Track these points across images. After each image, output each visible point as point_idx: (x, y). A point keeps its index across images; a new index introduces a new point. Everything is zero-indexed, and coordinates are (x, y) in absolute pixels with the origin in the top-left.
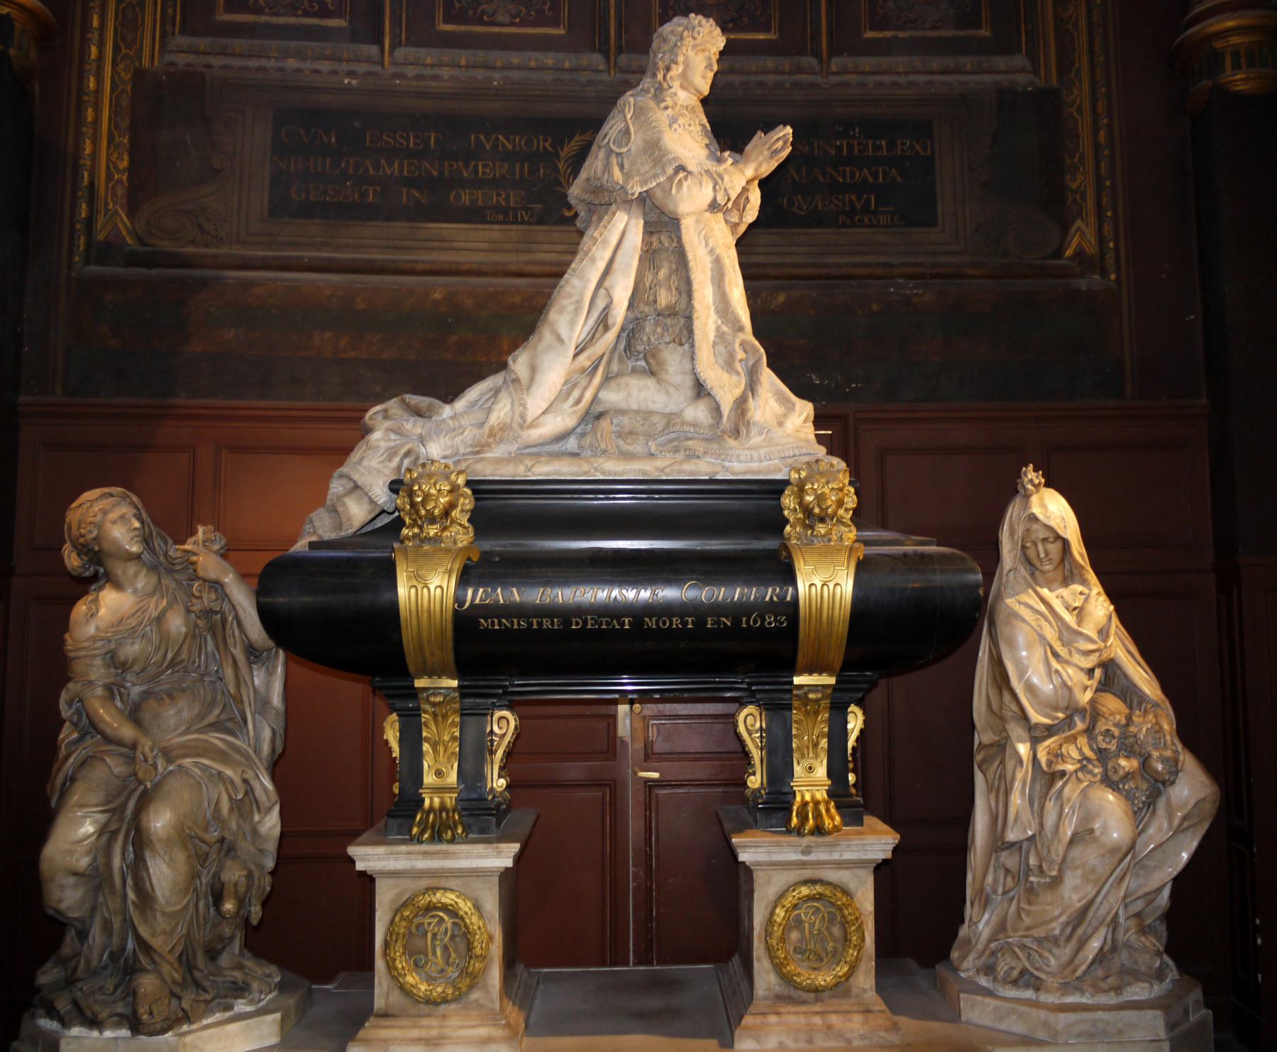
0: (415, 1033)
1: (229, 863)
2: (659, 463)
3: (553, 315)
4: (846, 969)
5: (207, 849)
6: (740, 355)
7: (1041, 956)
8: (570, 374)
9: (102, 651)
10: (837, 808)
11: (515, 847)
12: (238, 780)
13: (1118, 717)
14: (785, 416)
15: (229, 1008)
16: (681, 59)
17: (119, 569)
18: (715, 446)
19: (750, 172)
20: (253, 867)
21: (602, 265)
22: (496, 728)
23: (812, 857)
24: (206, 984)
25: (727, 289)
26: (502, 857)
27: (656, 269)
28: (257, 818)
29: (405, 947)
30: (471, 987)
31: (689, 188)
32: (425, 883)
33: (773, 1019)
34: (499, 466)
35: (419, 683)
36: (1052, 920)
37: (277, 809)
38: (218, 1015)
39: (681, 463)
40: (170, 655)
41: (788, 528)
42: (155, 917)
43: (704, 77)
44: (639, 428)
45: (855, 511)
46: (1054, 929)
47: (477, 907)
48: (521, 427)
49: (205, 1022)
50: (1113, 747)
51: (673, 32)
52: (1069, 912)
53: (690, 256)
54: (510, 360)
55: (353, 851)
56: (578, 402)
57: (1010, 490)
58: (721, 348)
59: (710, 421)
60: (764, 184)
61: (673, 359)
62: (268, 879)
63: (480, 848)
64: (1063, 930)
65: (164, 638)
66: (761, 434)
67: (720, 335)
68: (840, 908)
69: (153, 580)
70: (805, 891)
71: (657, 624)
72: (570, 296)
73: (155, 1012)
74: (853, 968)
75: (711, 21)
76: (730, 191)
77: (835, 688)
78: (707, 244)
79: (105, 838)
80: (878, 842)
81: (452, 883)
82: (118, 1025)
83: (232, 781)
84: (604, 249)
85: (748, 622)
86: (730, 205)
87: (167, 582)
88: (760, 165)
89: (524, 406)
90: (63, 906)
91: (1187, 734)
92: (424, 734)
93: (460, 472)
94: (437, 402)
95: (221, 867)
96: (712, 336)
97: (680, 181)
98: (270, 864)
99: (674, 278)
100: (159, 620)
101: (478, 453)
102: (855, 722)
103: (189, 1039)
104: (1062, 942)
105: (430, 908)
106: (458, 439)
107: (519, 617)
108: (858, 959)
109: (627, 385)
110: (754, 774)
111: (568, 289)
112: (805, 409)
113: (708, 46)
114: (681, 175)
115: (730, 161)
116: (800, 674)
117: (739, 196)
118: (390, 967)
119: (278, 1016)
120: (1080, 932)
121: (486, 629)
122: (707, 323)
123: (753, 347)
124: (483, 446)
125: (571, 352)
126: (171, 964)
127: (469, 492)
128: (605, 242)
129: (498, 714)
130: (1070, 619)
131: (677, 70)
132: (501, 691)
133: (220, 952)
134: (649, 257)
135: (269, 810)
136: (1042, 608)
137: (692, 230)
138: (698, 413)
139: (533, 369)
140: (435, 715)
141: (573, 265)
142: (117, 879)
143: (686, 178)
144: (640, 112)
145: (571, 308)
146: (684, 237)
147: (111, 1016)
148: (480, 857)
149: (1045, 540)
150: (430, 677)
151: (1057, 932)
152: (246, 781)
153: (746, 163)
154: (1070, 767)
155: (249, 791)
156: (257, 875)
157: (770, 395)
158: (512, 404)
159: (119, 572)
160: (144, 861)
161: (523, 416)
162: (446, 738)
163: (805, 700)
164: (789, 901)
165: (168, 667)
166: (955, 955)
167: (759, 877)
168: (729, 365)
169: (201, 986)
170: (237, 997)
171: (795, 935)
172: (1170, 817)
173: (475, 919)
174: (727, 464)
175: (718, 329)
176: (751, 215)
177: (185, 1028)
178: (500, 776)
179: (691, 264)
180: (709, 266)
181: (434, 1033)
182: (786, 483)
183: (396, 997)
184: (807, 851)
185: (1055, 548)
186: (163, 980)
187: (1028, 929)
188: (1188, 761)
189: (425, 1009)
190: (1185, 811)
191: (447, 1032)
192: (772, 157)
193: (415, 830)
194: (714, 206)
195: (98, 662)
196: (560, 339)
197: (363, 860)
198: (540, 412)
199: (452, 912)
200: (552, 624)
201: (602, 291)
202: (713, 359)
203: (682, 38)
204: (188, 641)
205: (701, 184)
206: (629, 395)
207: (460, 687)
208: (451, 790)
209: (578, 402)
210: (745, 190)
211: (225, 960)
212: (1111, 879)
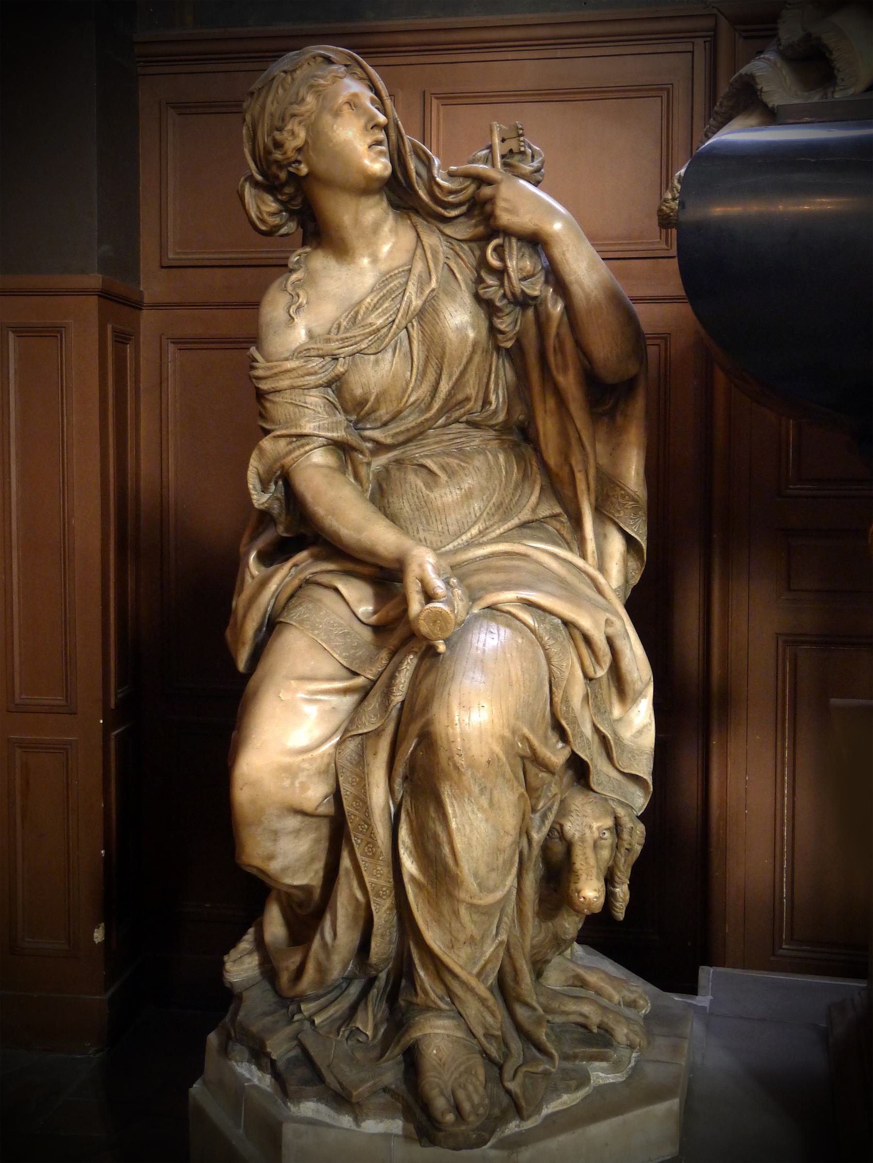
1: (579, 802)
9: (322, 378)
20: (621, 812)
24: (542, 1034)
38: (565, 1097)
40: (444, 387)
65: (435, 351)
69: (407, 237)
82: (384, 1112)
87: (431, 239)
95: (564, 811)
100: (427, 314)
126: (482, 1001)
147: (374, 1093)
159: (347, 219)
165: (440, 413)
195: (314, 399)
204: (477, 358)
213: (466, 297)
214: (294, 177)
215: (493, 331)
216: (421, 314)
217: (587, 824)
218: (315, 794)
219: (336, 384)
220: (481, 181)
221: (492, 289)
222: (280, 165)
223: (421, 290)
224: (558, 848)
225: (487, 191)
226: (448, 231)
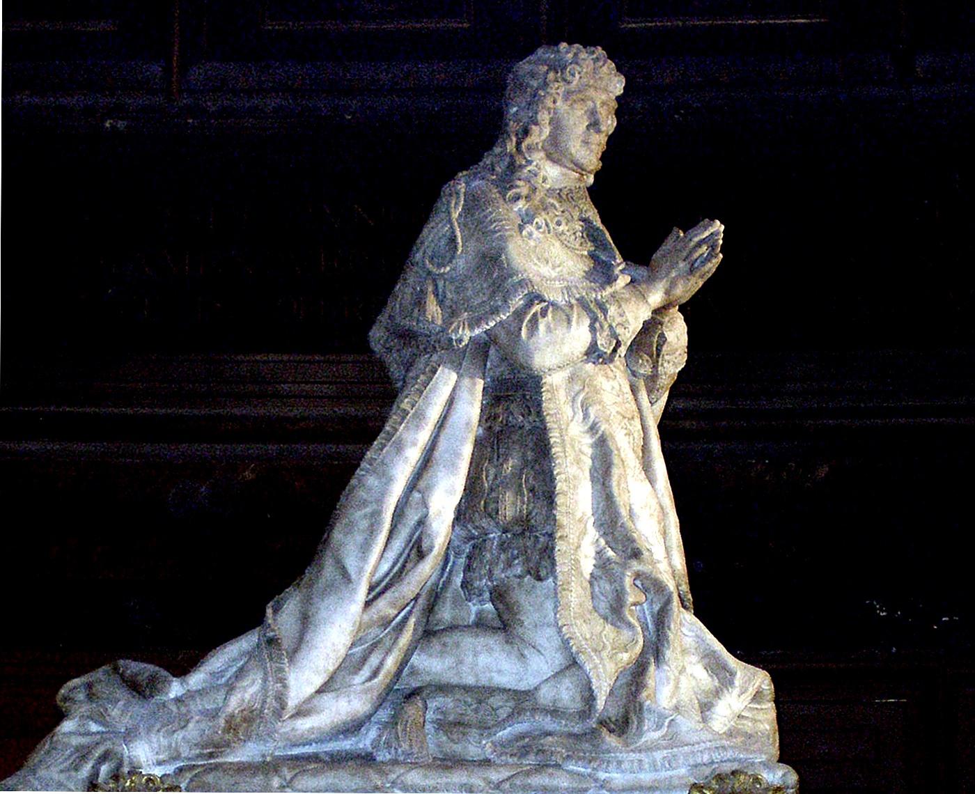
3: (337, 535)
8: (361, 627)
14: (717, 693)
16: (544, 117)
18: (586, 746)
19: (656, 297)
21: (413, 455)
25: (615, 491)
27: (502, 458)
31: (549, 329)
39: (528, 774)
43: (586, 143)
44: (471, 716)
51: (533, 75)
56: (375, 674)
60: (689, 310)
66: (659, 727)
67: (603, 565)
72: (365, 503)
75: (600, 51)
76: (619, 330)
88: (673, 284)
89: (282, 681)
94: (165, 673)
97: (535, 315)
101: (211, 756)
106: (179, 736)
109: (457, 645)
111: (362, 494)
113: (591, 93)
114: (537, 308)
115: (623, 280)
122: (580, 544)
124: (217, 746)
125: (361, 594)
128: (420, 416)
131: (540, 135)
134: (492, 441)
137: (562, 395)
139: (306, 621)
141: (369, 455)
143: (544, 313)
144: (474, 204)
145: (364, 524)
153: (651, 280)
158: (265, 680)
161: (281, 699)
168: (615, 611)
174: (602, 775)
175: (599, 553)
180: (589, 451)
192: (692, 271)
194: (593, 353)
198: (310, 690)
202: (589, 605)
203: (545, 84)
205: (569, 321)
206: (461, 662)
209: (375, 674)
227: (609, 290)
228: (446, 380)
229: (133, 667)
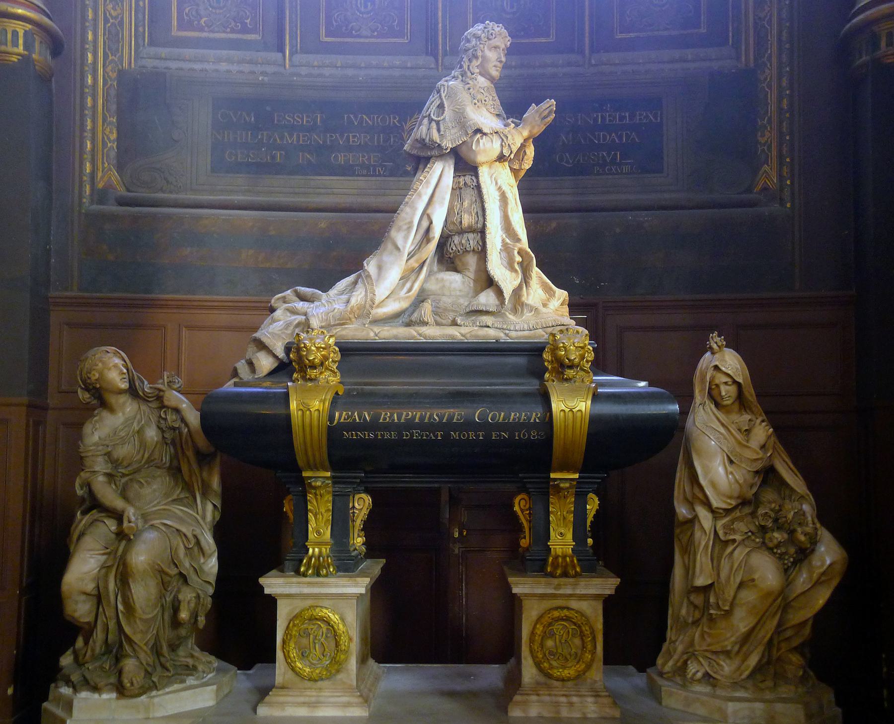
0: (302, 699)
2: (464, 330)
3: (393, 233)
4: (583, 666)
5: (170, 577)
6: (518, 259)
7: (718, 664)
8: (405, 271)
9: (103, 453)
10: (578, 560)
11: (367, 581)
12: (190, 535)
13: (773, 505)
15: (183, 681)
17: (112, 399)
20: (200, 592)
21: (425, 199)
22: (356, 505)
23: (561, 592)
24: (168, 665)
25: (510, 214)
26: (357, 586)
28: (202, 561)
29: (295, 643)
30: (338, 671)
32: (309, 603)
33: (534, 698)
34: (358, 332)
35: (305, 474)
36: (727, 639)
37: (216, 554)
41: (547, 375)
42: (135, 622)
45: (593, 362)
46: (727, 646)
47: (343, 619)
48: (372, 307)
49: (167, 690)
50: (769, 524)
52: (738, 634)
53: (484, 191)
54: (365, 263)
55: (262, 581)
56: (410, 290)
57: (702, 348)
58: (504, 254)
59: (497, 302)
61: (472, 261)
62: (210, 599)
63: (344, 581)
64: (733, 647)
65: (143, 444)
67: (505, 245)
68: (579, 627)
70: (556, 614)
71: (459, 436)
73: (135, 682)
74: (589, 667)
77: (579, 482)
78: (496, 183)
79: (104, 571)
80: (608, 585)
81: (326, 603)
82: (111, 691)
83: (185, 535)
84: (427, 187)
85: (519, 436)
86: (512, 156)
87: (144, 407)
90: (76, 615)
91: (823, 517)
92: (309, 507)
93: (331, 336)
95: (179, 591)
96: (499, 245)
98: (211, 590)
99: (474, 206)
100: (140, 432)
102: (593, 505)
103: (156, 700)
104: (732, 655)
105: (313, 619)
107: (369, 431)
108: (592, 660)
110: (525, 538)
111: (403, 215)
112: (562, 295)
116: (555, 472)
117: (519, 150)
118: (286, 657)
119: (215, 687)
120: (745, 649)
121: (348, 439)
123: (527, 253)
125: (405, 257)
126: (146, 652)
127: (337, 349)
128: (428, 183)
129: (357, 497)
130: (739, 436)
132: (358, 481)
133: (178, 646)
135: (210, 556)
136: (722, 430)
138: (487, 299)
139: (380, 268)
140: (316, 494)
142: (112, 598)
145: (405, 227)
146: (481, 178)
148: (344, 586)
149: (726, 383)
150: (312, 470)
151: (729, 648)
152: (195, 536)
154: (738, 537)
155: (198, 543)
156: (202, 596)
157: (538, 286)
158: (366, 291)
160: (129, 587)
162: (323, 511)
163: (558, 489)
164: (546, 620)
165: (145, 463)
166: (660, 661)
167: (526, 604)
169: (163, 670)
170: (188, 675)
171: (550, 643)
172: (811, 572)
173: (341, 626)
175: (503, 240)
176: (528, 164)
177: (154, 693)
178: (359, 536)
179: (485, 197)
181: (313, 699)
182: (548, 343)
183: (290, 674)
184: (558, 587)
185: (732, 390)
186: (141, 663)
187: (709, 645)
188: (825, 535)
189: (309, 684)
190: (822, 570)
191: (322, 699)
193: (302, 569)
194: (501, 158)
195: (100, 459)
196: (398, 249)
197: (269, 587)
199: (328, 622)
200: (391, 435)
201: (425, 217)
207: (333, 477)
208: (326, 544)
209: (410, 290)
210: (523, 146)
211: (181, 652)
212: (767, 614)
213: (154, 427)
214: (95, 388)
215: (163, 437)
216: (138, 432)
217: (187, 595)
218: (90, 587)
219: (108, 454)
220: (160, 390)
221: (163, 424)
222: (90, 384)
223: (139, 423)
224: (176, 604)
225: (161, 393)
226: (150, 405)
227: (508, 129)
228: (437, 168)
229: (302, 289)
